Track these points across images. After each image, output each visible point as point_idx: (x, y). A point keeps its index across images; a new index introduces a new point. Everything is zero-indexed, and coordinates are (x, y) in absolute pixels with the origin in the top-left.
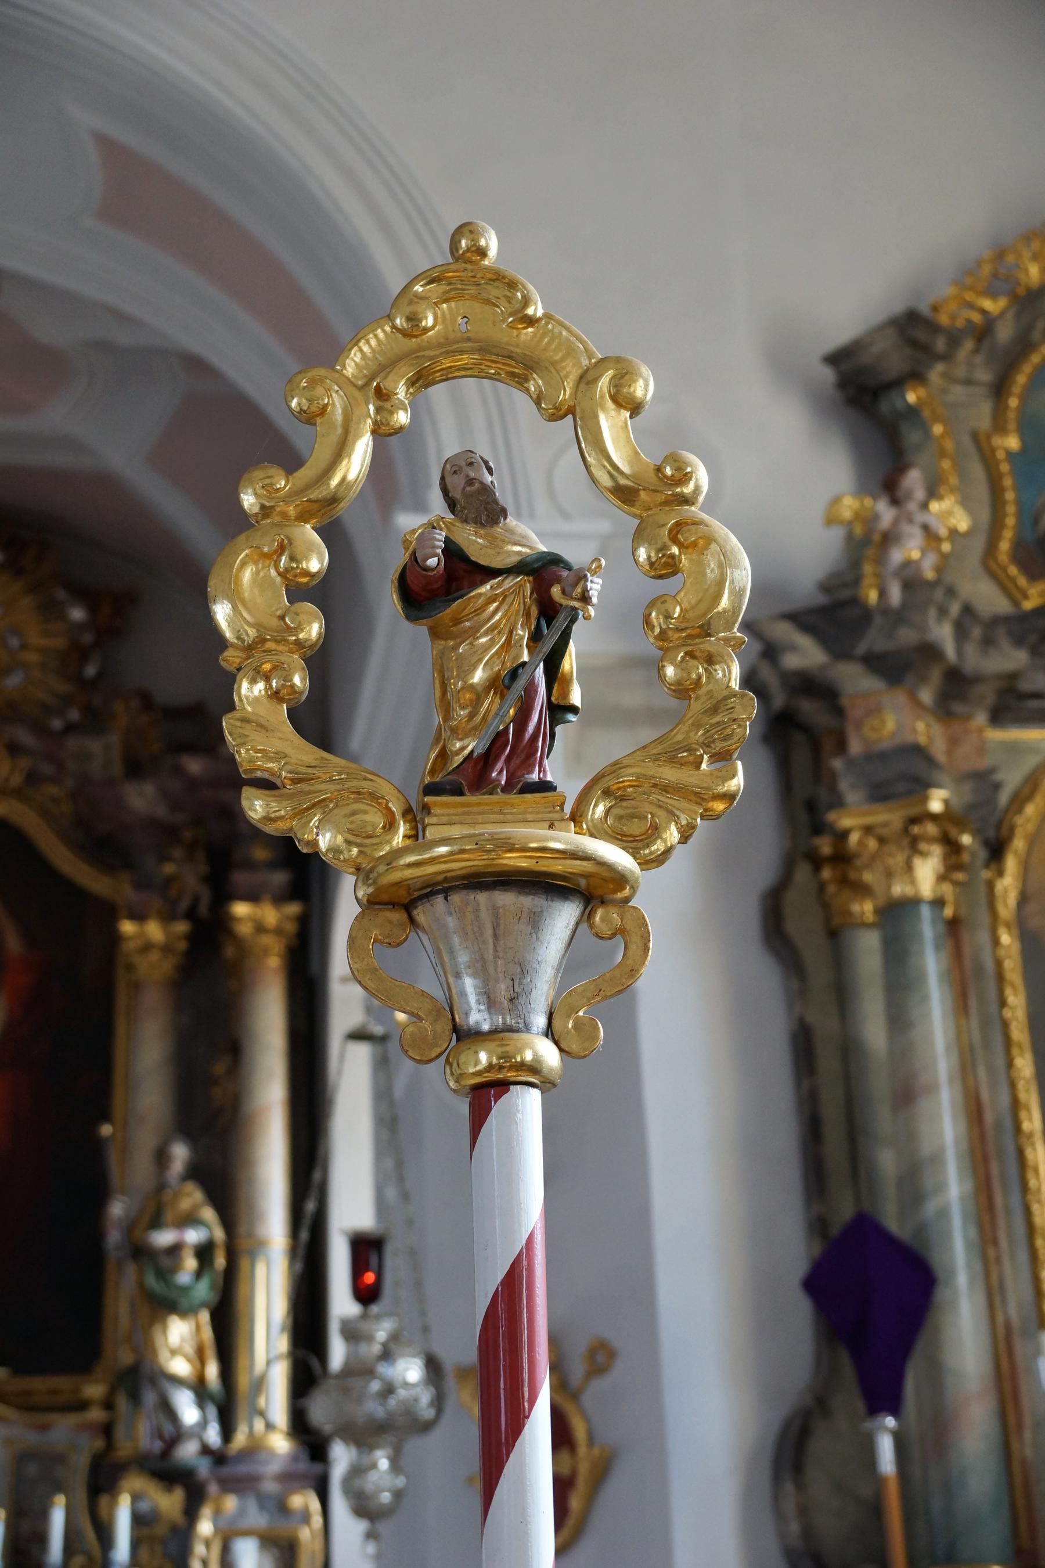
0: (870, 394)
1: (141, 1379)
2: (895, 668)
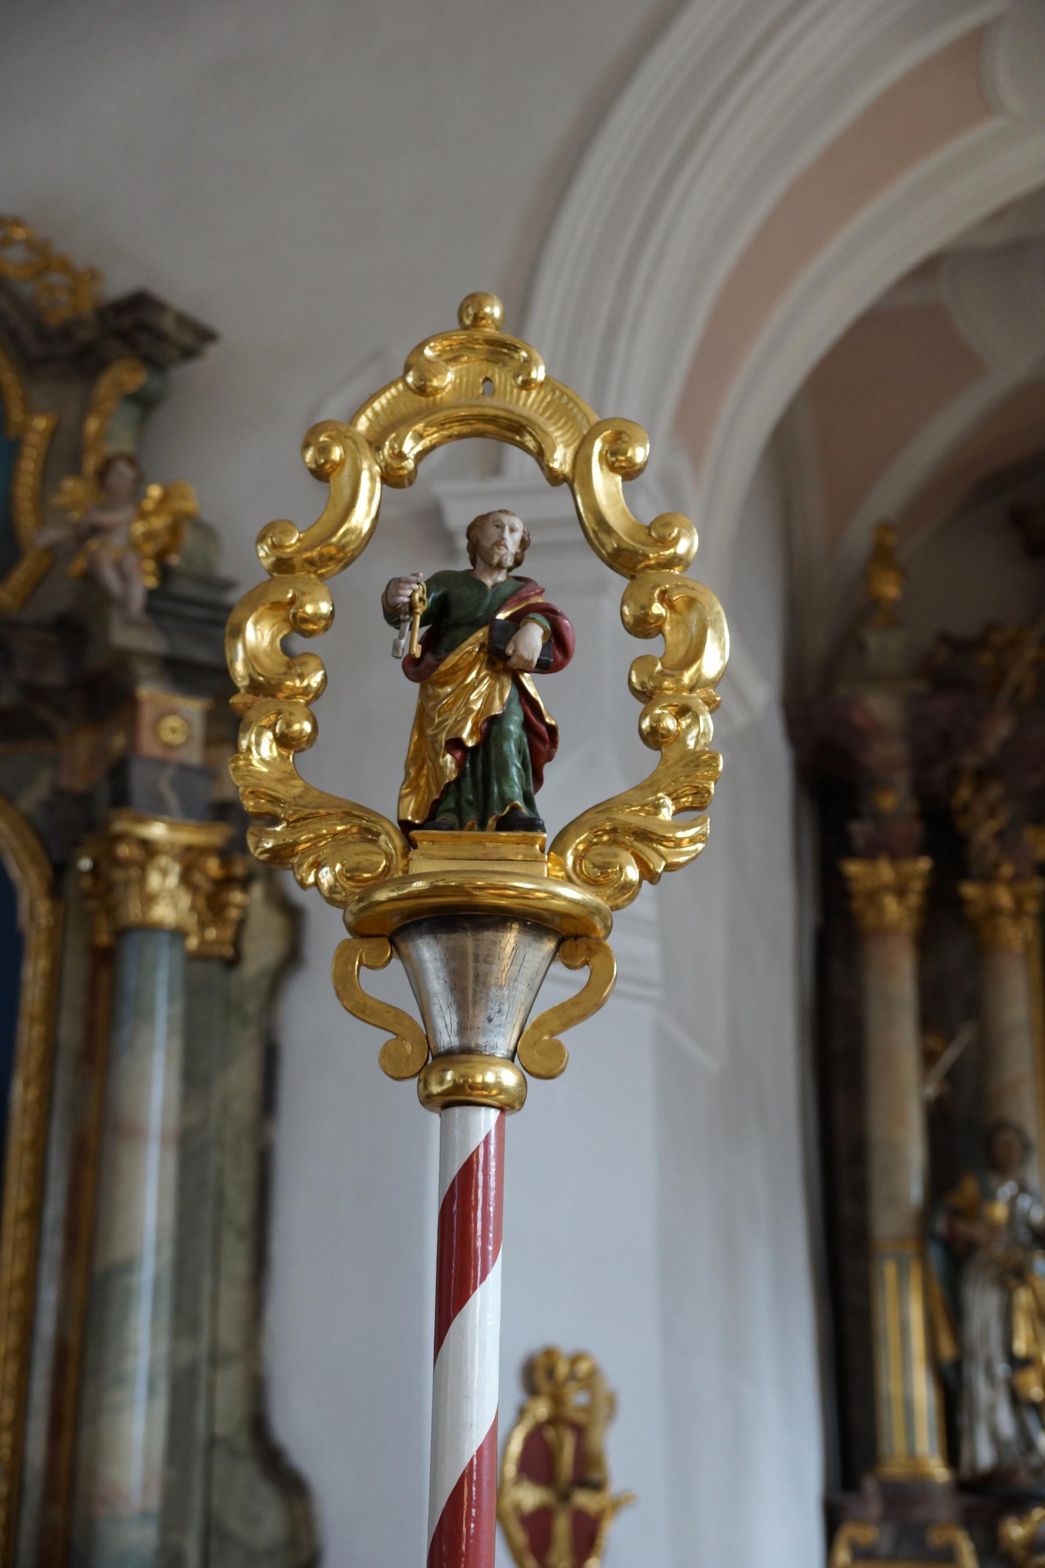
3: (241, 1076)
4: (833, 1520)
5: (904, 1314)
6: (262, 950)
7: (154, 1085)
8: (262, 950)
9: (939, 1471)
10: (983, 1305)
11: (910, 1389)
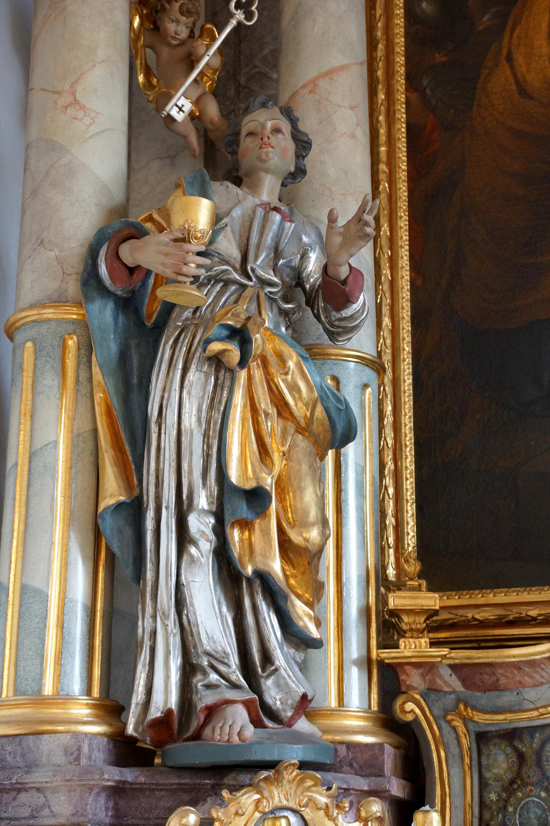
9: (83, 719)
10: (181, 398)
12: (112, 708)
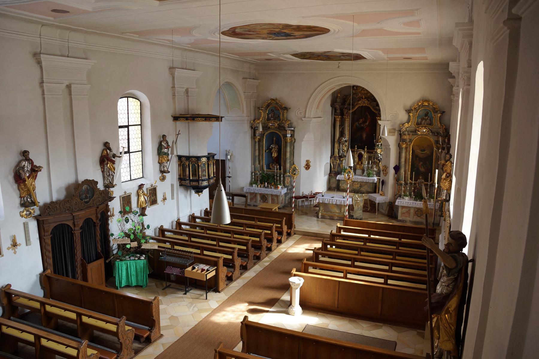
0: (409, 111)
1: (376, 152)
2: (405, 134)
3: (292, 147)
4: (331, 158)
5: (336, 145)
6: (293, 141)
7: (288, 149)
8: (293, 141)
10: (341, 146)
11: (336, 150)
12: (339, 154)
